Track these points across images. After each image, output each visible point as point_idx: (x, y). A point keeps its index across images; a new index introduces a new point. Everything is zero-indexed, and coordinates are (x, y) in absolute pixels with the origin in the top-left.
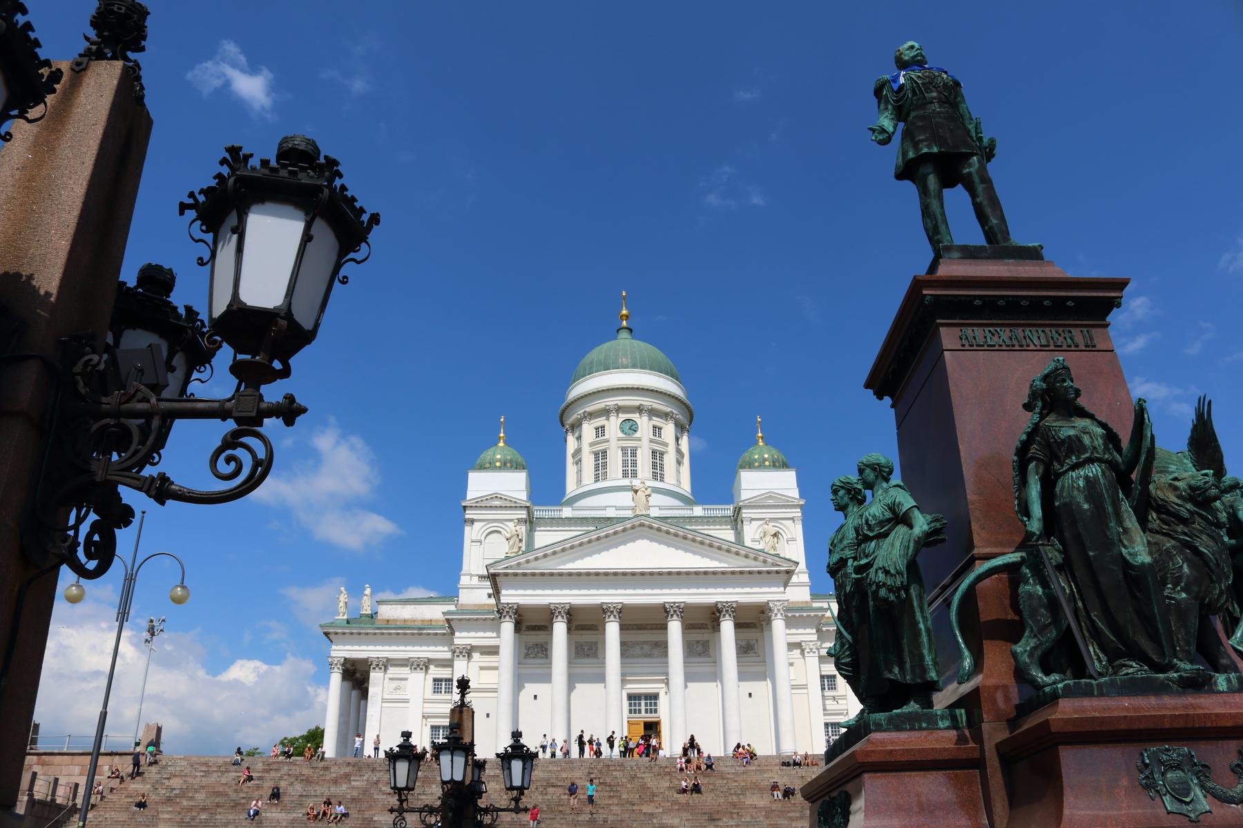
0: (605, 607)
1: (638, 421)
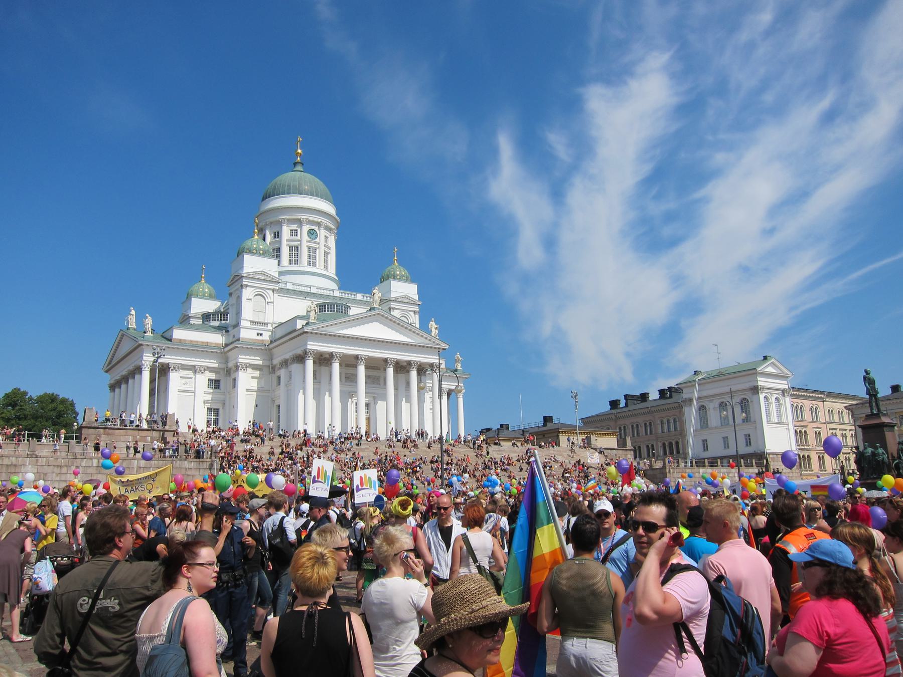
0: (359, 356)
1: (317, 231)
